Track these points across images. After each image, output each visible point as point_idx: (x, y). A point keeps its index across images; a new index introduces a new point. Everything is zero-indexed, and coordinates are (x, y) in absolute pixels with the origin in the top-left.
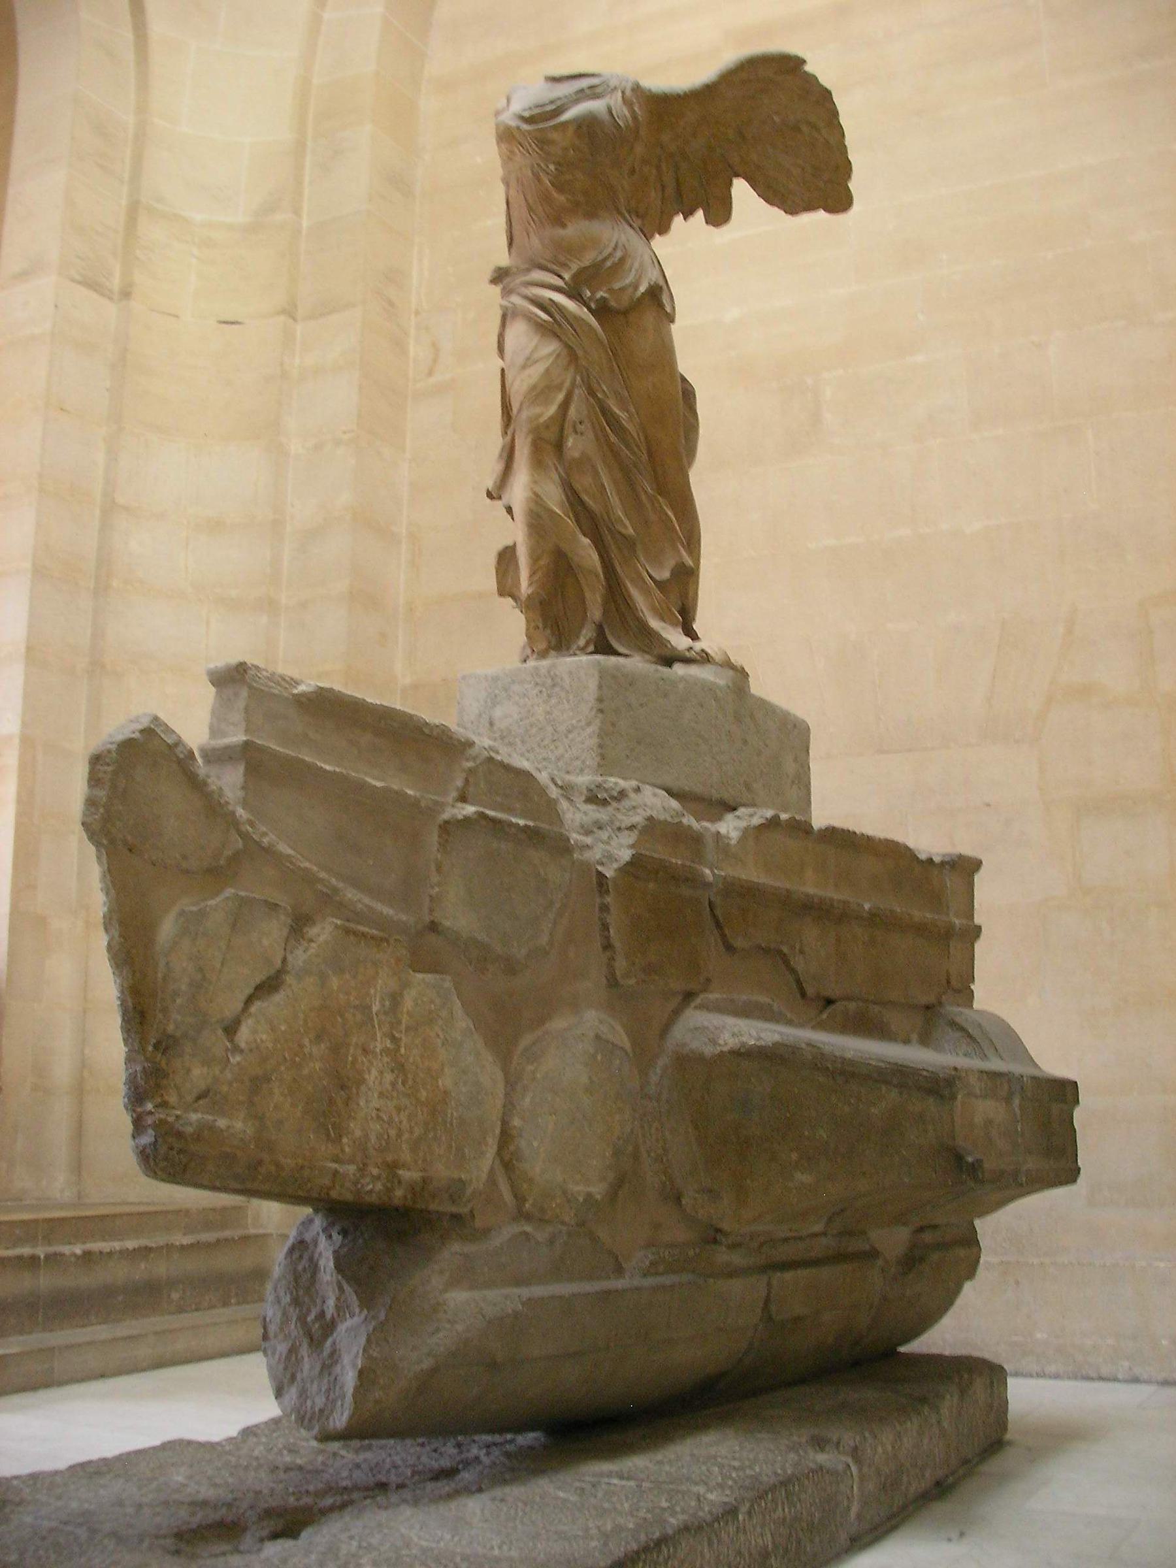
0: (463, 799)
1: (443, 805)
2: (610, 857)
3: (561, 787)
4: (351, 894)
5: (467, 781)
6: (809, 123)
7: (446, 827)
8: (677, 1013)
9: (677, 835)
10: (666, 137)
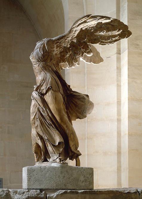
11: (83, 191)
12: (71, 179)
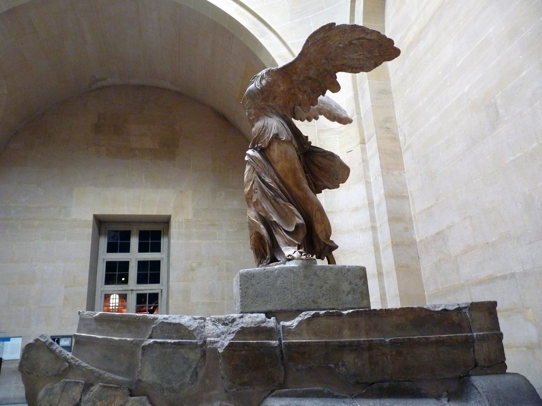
0: (151, 337)
1: (143, 341)
2: (222, 345)
3: (214, 321)
4: (107, 374)
5: (152, 332)
6: (356, 39)
7: (144, 348)
8: (265, 398)
9: (258, 331)
10: (295, 77)
11: (351, 311)
12: (324, 288)
